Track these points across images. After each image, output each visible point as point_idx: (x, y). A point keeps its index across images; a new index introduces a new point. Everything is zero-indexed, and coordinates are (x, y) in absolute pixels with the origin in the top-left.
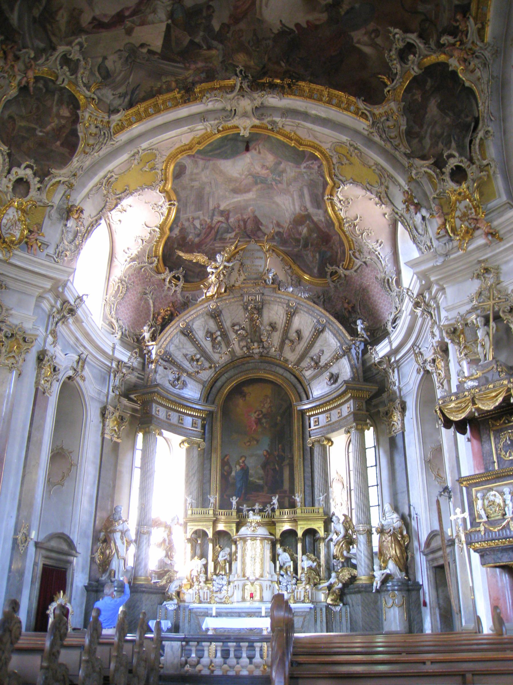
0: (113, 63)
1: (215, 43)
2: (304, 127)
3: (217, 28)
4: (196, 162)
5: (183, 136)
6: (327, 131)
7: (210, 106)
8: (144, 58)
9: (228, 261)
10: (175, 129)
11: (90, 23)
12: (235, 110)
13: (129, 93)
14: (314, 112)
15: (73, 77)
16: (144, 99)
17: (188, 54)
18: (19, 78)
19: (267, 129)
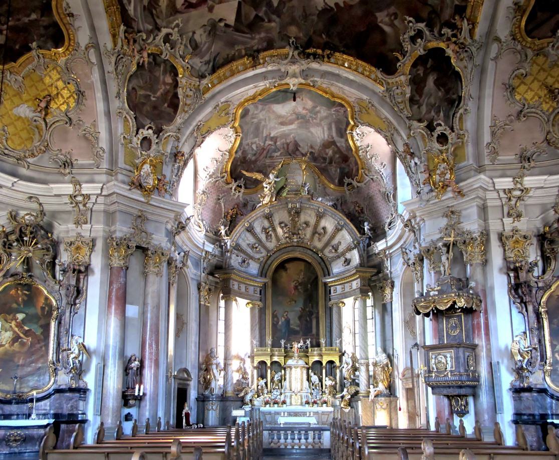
0: (201, 36)
2: (337, 86)
4: (257, 107)
5: (249, 90)
6: (353, 91)
7: (270, 68)
9: (277, 178)
10: (244, 86)
11: (183, 5)
13: (212, 60)
14: (344, 75)
15: (173, 50)
16: (222, 65)
17: (253, 26)
19: (309, 85)
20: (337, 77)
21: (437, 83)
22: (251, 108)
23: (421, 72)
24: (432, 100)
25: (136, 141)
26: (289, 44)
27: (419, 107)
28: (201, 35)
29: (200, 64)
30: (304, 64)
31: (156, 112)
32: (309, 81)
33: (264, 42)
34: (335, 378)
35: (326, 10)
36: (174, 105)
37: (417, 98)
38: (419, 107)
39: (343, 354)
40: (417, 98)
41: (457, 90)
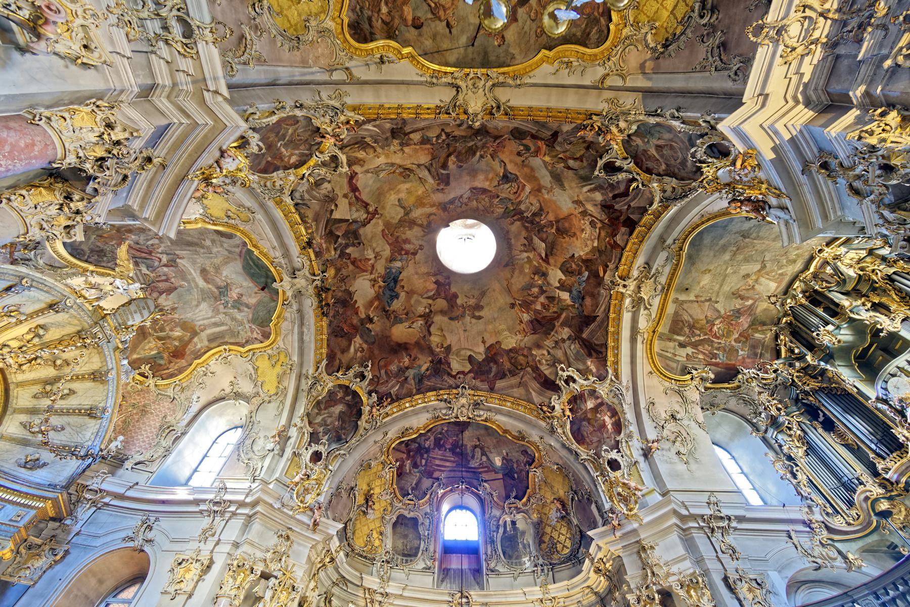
1: (338, 252)
3: (347, 251)
20: (302, 324)
21: (341, 416)
24: (329, 421)
27: (317, 414)
37: (323, 406)
38: (317, 414)
40: (323, 406)
41: (348, 435)
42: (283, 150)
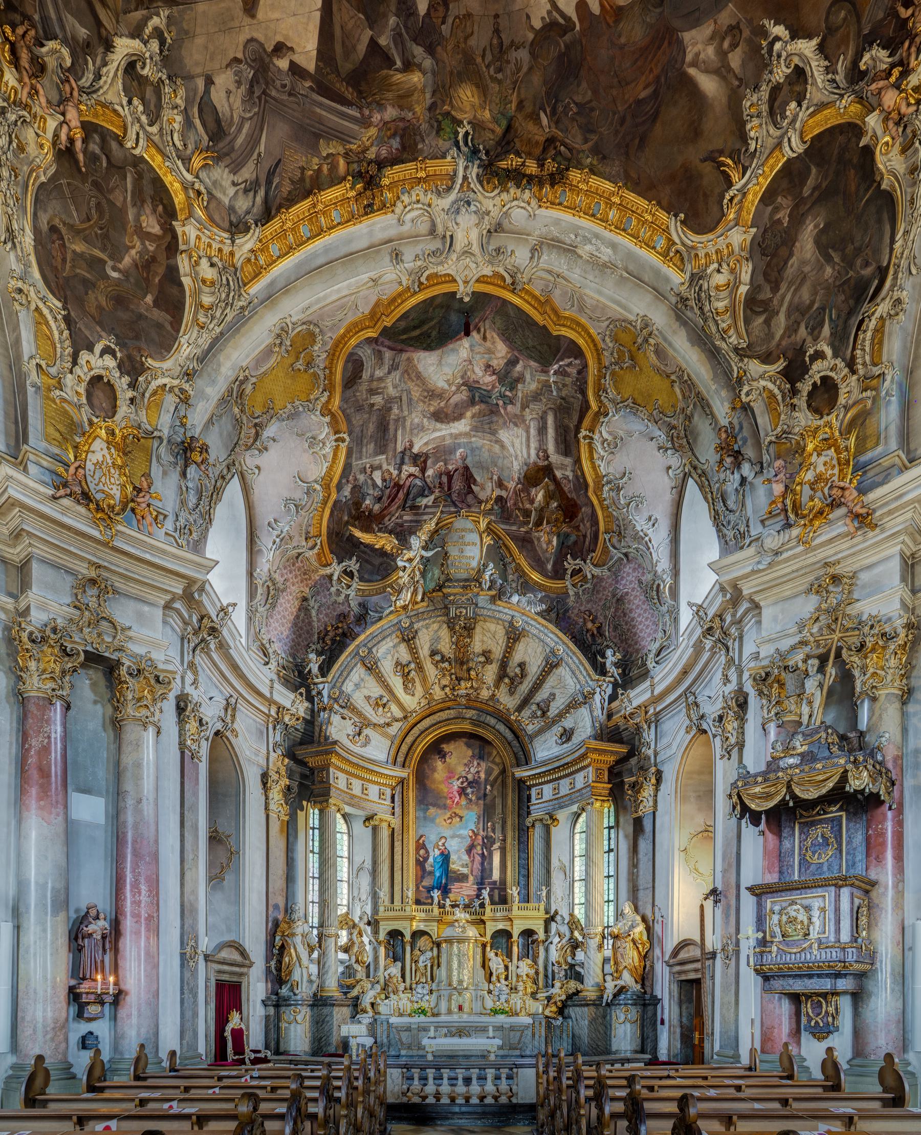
8: (284, 86)
12: (451, 236)
18: (52, 124)
22: (366, 354)
23: (783, 216)
25: (74, 387)
26: (457, 144)
28: (229, 92)
29: (231, 191)
30: (492, 202)
31: (123, 315)
32: (501, 270)
33: (394, 135)
34: (535, 962)
35: (555, 27)
36: (172, 301)
38: (767, 322)
39: (553, 919)
42: (127, 260)
